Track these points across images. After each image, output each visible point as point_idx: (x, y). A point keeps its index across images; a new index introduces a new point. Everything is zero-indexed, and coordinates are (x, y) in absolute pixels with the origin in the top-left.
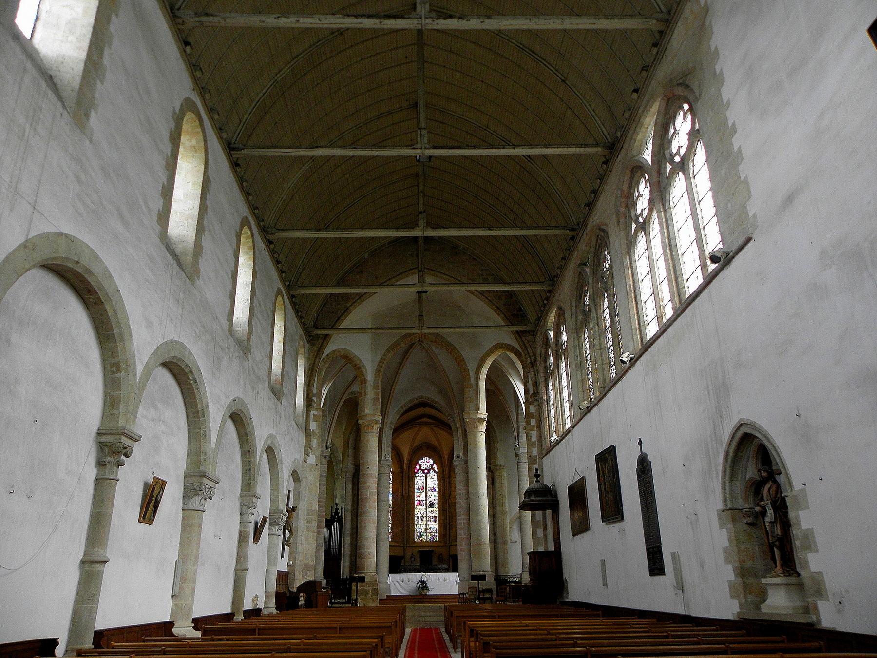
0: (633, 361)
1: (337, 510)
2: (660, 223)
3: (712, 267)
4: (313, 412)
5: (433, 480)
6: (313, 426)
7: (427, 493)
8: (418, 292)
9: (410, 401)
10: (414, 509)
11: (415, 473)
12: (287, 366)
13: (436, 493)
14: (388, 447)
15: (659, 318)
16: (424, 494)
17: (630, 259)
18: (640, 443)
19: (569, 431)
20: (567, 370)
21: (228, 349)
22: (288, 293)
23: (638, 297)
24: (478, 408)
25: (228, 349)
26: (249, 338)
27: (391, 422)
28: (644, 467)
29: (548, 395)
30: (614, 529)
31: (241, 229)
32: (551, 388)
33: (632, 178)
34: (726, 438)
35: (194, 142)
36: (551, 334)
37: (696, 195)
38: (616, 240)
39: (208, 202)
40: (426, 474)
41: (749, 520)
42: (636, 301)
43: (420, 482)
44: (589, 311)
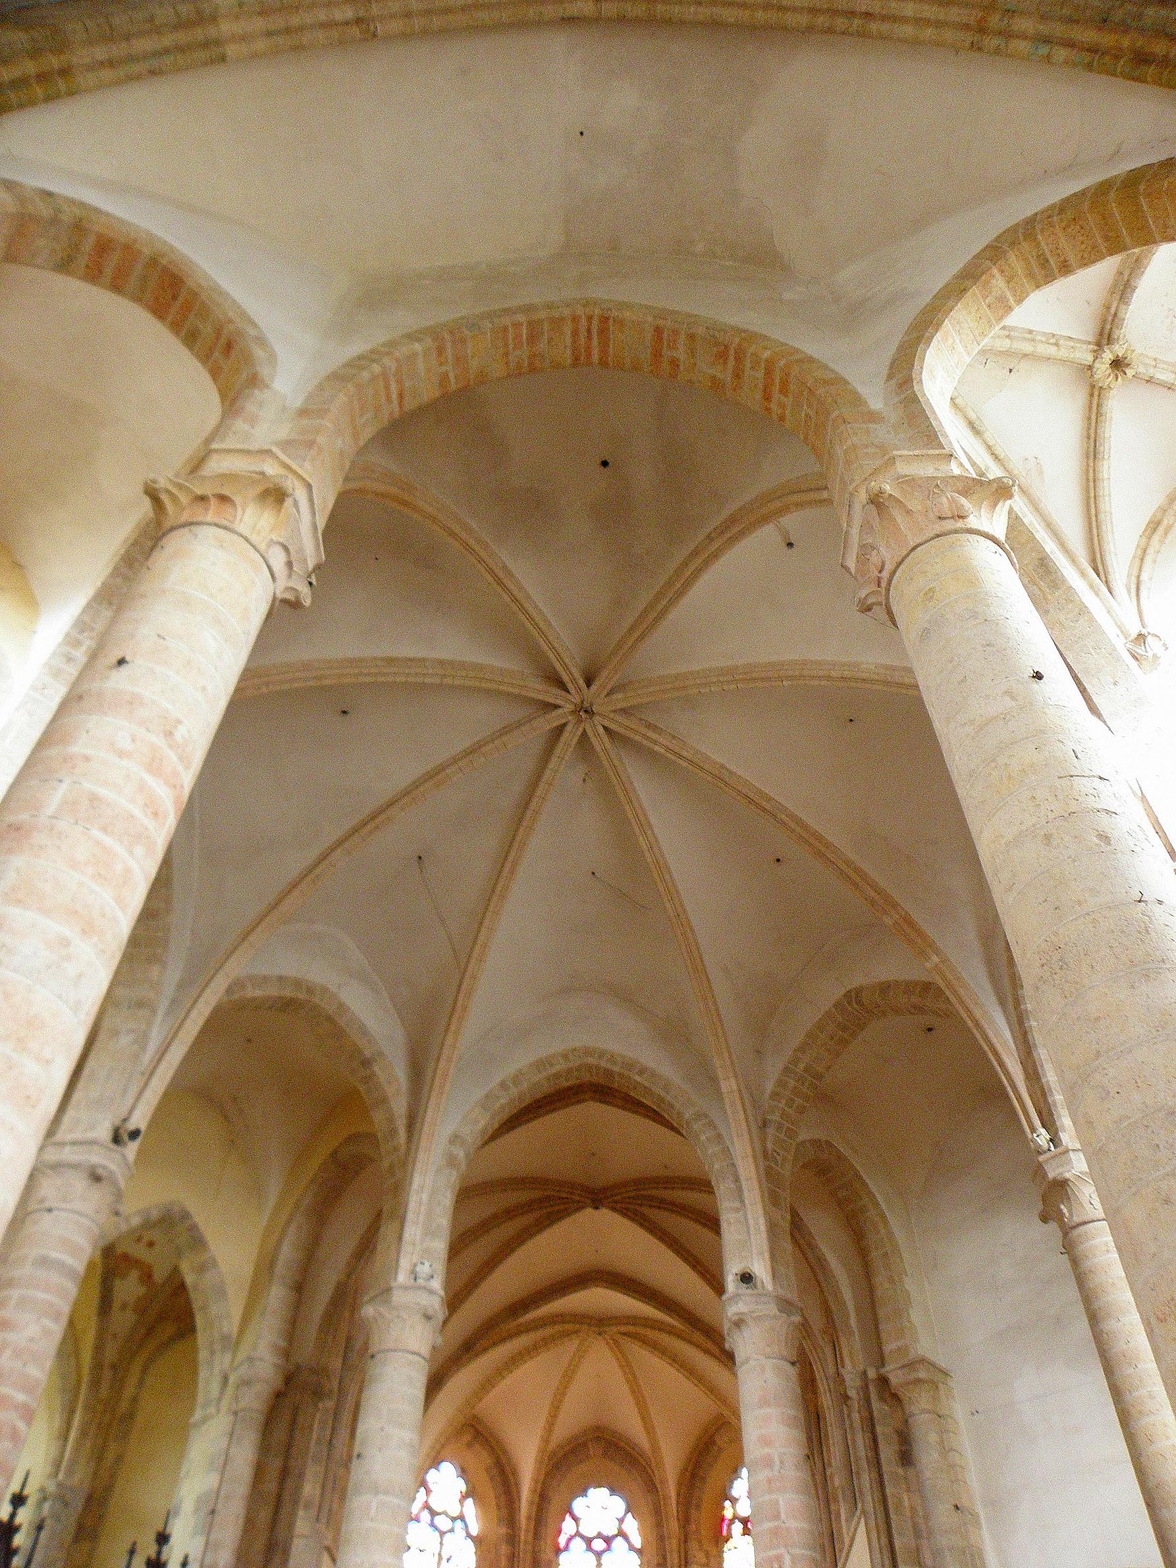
9: (539, 1065)
11: (558, 1551)
14: (429, 1233)
27: (455, 1139)
40: (599, 1555)
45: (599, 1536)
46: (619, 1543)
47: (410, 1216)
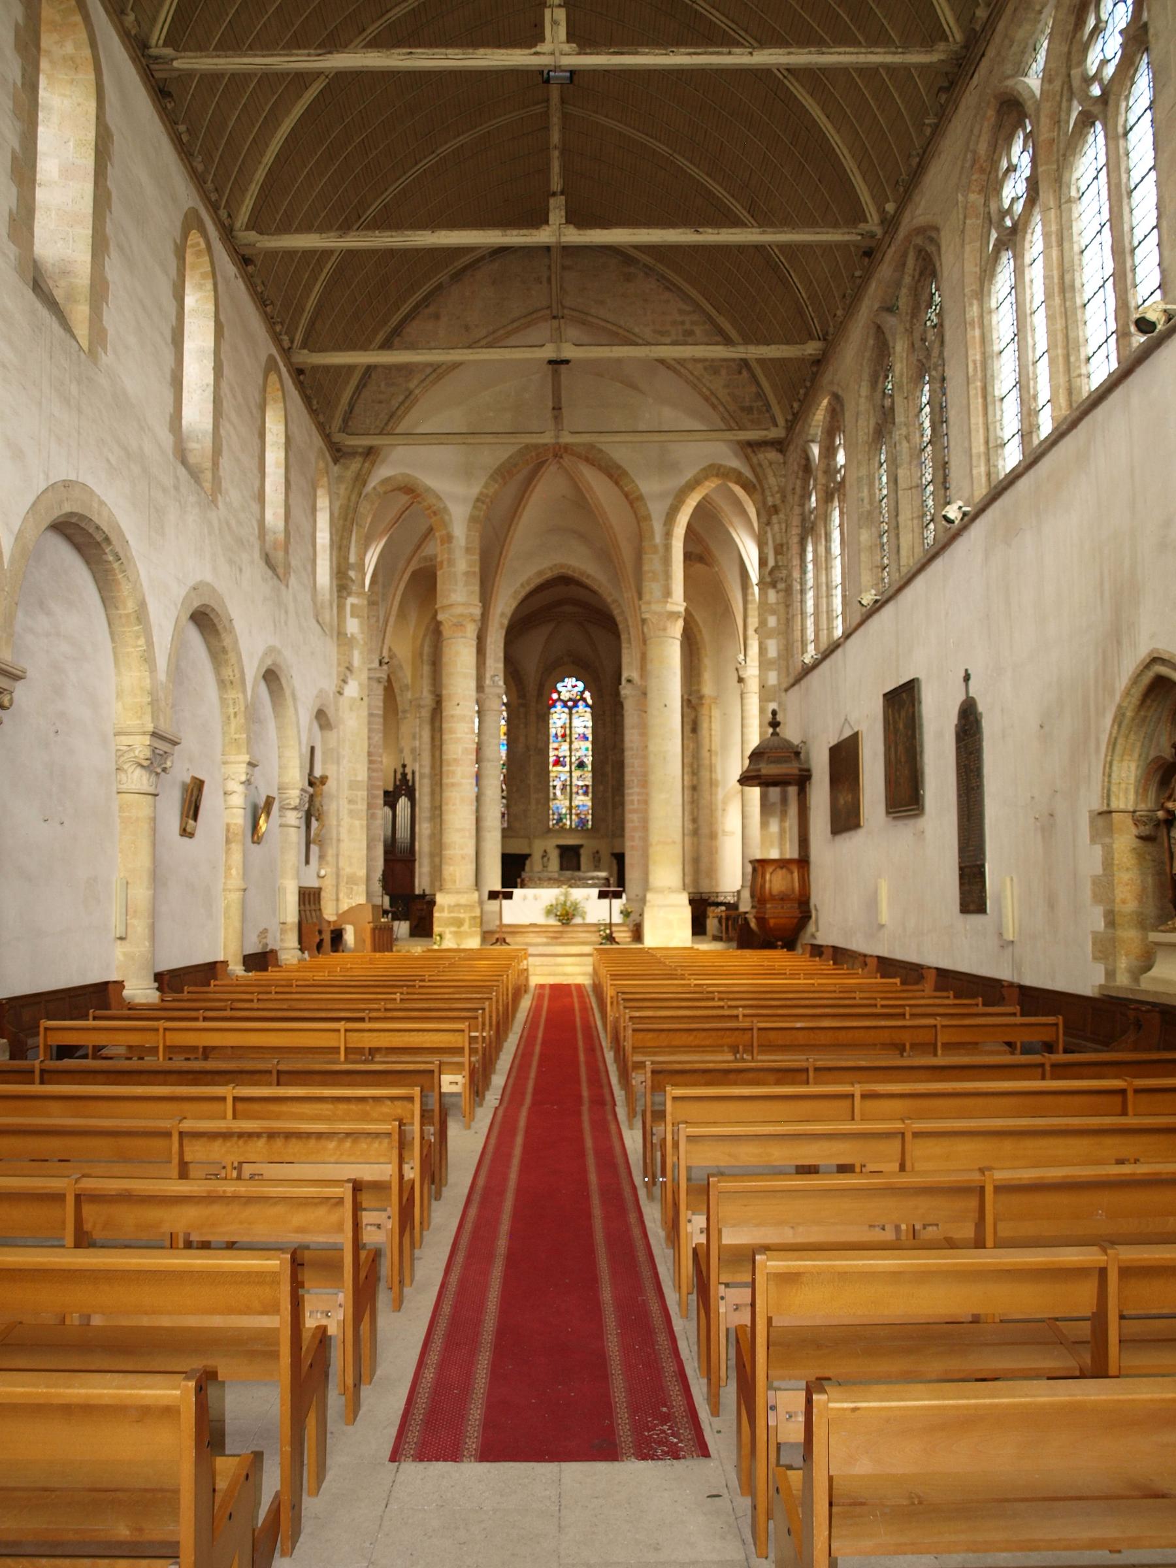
0: (969, 519)
1: (404, 775)
2: (1046, 235)
3: (1139, 339)
4: (351, 600)
5: (583, 722)
6: (353, 626)
7: (571, 743)
8: (550, 362)
9: (540, 573)
10: (548, 772)
12: (296, 512)
13: (589, 745)
15: (1026, 434)
16: (565, 746)
17: (981, 306)
18: (967, 678)
19: (835, 647)
20: (841, 525)
21: (177, 488)
22: (289, 364)
23: (989, 389)
24: (668, 593)
25: (177, 488)
26: (215, 464)
27: (503, 614)
28: (969, 725)
29: (803, 571)
30: (905, 831)
31: (185, 236)
32: (810, 556)
33: (999, 126)
34: (1122, 682)
35: (69, 48)
36: (815, 450)
37: (1124, 176)
38: (956, 261)
39: (110, 184)
40: (570, 709)
41: (1146, 830)
42: (985, 397)
43: (560, 723)
44: (892, 409)
45: (570, 700)
46: (581, 703)
47: (488, 655)
